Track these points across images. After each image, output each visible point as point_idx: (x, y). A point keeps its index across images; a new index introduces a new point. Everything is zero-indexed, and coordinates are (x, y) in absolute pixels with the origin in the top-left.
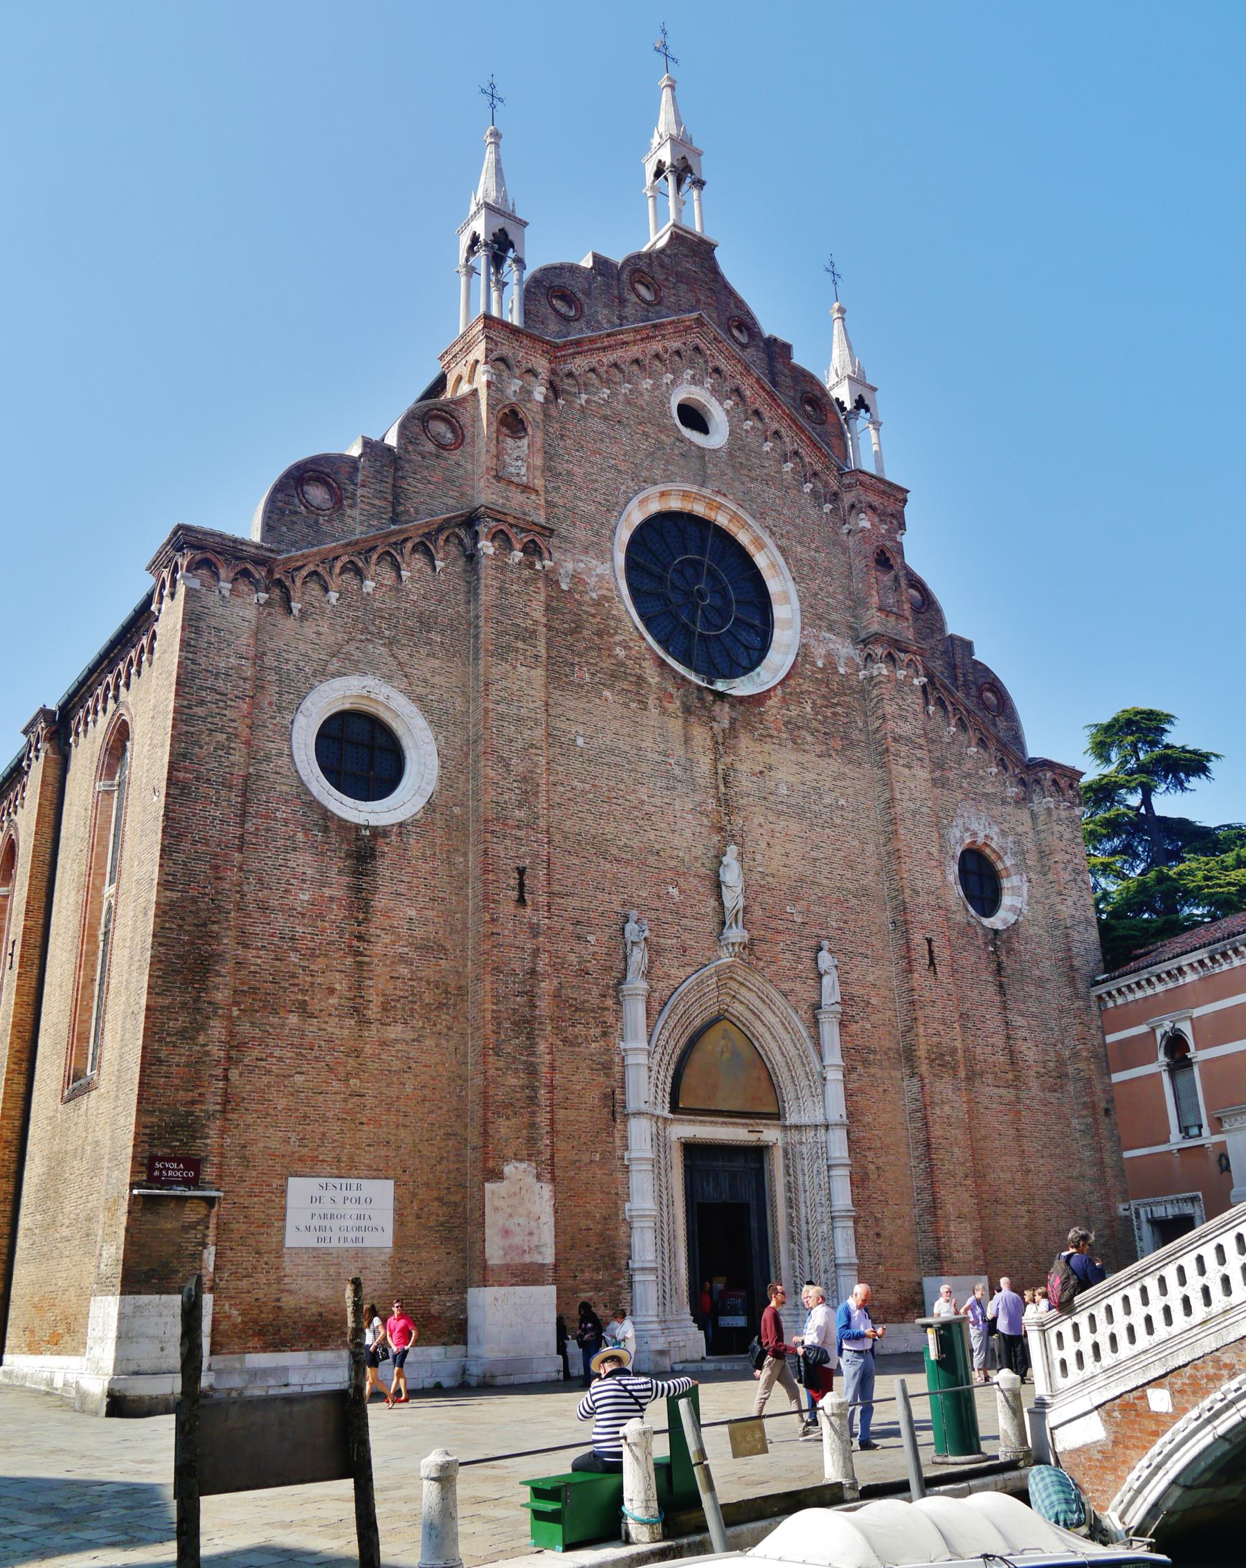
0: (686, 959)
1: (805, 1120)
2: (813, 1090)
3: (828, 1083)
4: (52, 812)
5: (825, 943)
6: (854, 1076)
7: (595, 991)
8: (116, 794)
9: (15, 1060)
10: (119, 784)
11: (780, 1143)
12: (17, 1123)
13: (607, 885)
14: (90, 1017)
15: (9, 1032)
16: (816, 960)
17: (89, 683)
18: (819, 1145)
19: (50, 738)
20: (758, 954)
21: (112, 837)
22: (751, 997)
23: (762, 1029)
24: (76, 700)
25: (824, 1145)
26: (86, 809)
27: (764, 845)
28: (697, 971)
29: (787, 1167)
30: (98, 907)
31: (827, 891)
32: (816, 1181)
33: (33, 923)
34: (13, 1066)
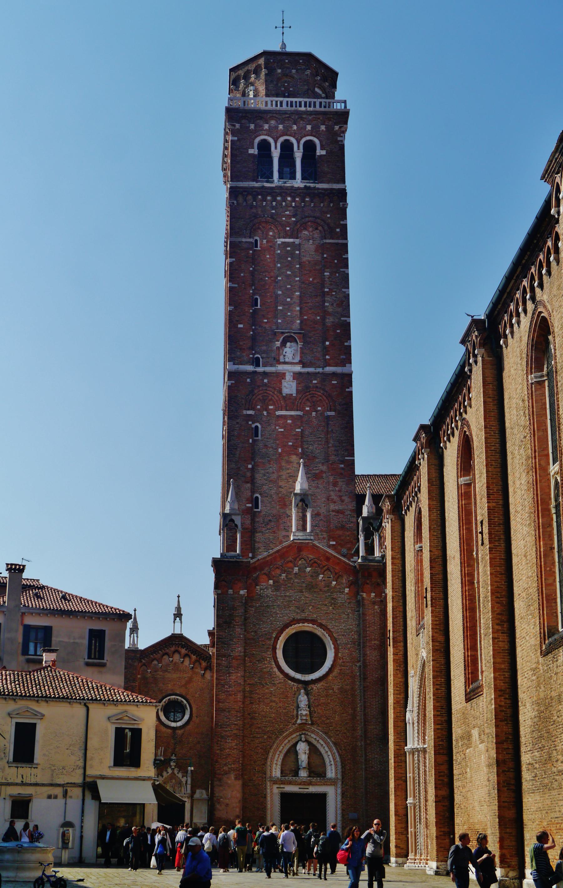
4: (495, 407)
8: (546, 383)
9: (498, 622)
10: (548, 375)
12: (507, 675)
14: (555, 581)
15: (490, 598)
17: (508, 290)
19: (483, 344)
21: (549, 421)
24: (499, 306)
26: (523, 400)
30: (547, 484)
33: (494, 504)
34: (497, 627)
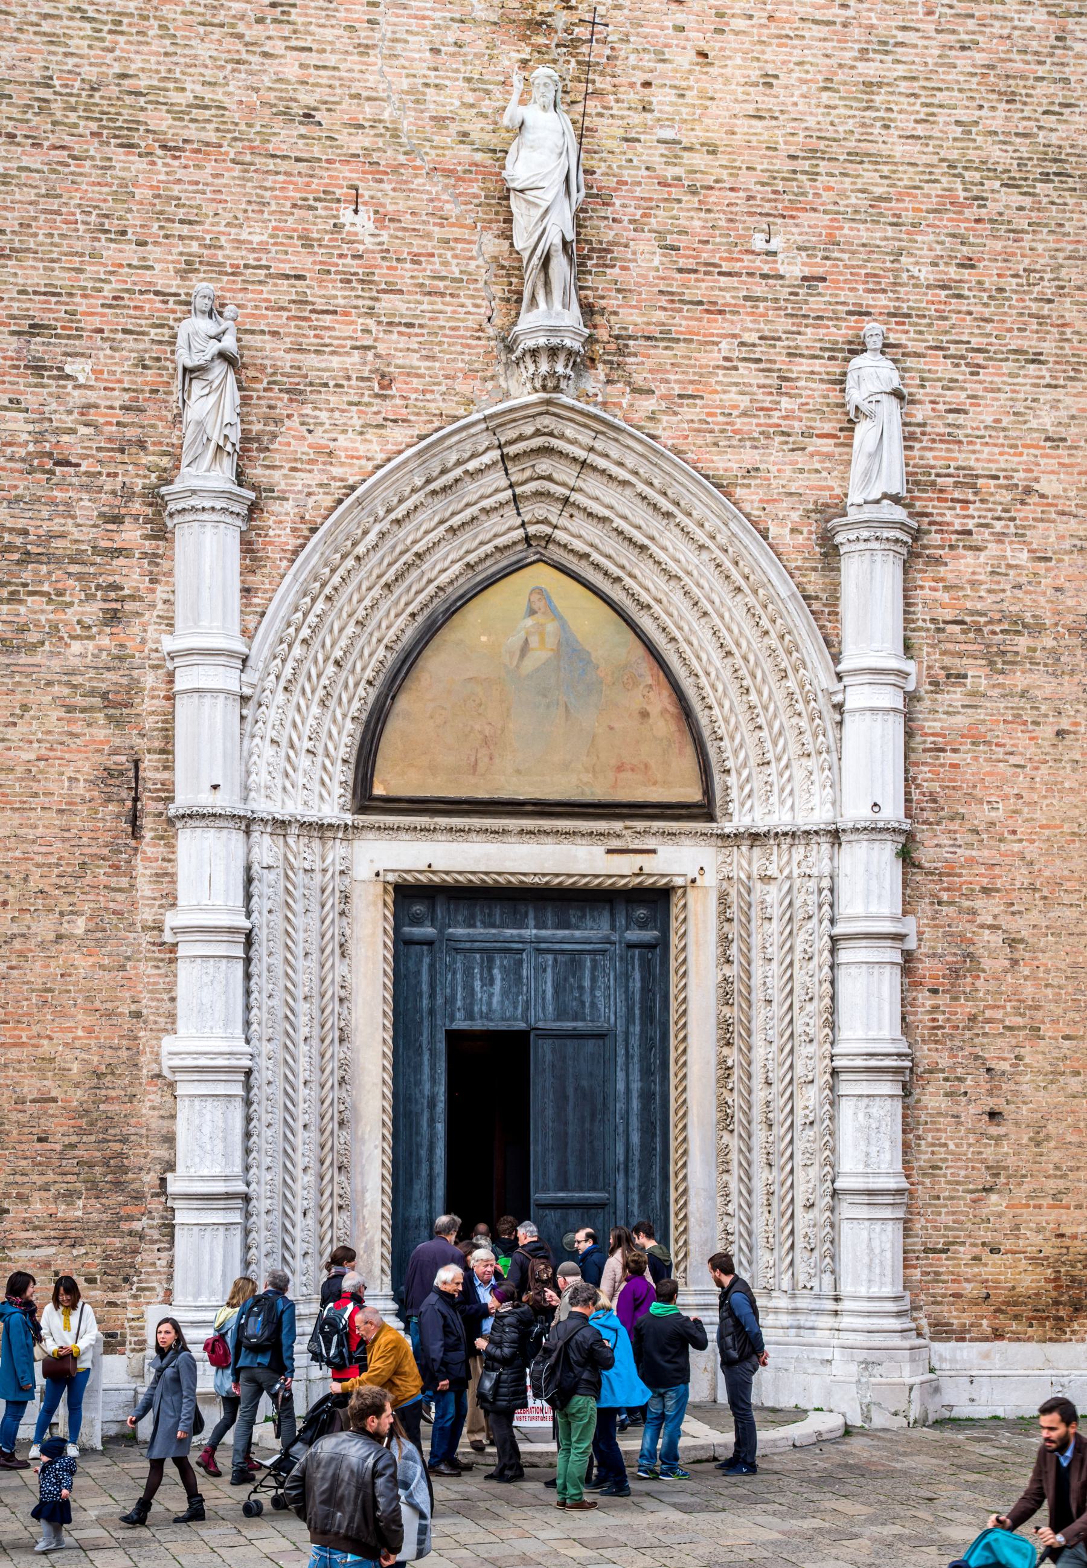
0: (388, 408)
1: (781, 819)
2: (807, 737)
3: (851, 723)
5: (872, 329)
6: (955, 696)
7: (87, 508)
11: (710, 880)
13: (133, 220)
16: (840, 381)
18: (812, 884)
20: (638, 380)
22: (610, 495)
23: (655, 582)
25: (826, 883)
27: (686, 59)
28: (422, 438)
29: (725, 941)
31: (907, 176)
32: (800, 977)
